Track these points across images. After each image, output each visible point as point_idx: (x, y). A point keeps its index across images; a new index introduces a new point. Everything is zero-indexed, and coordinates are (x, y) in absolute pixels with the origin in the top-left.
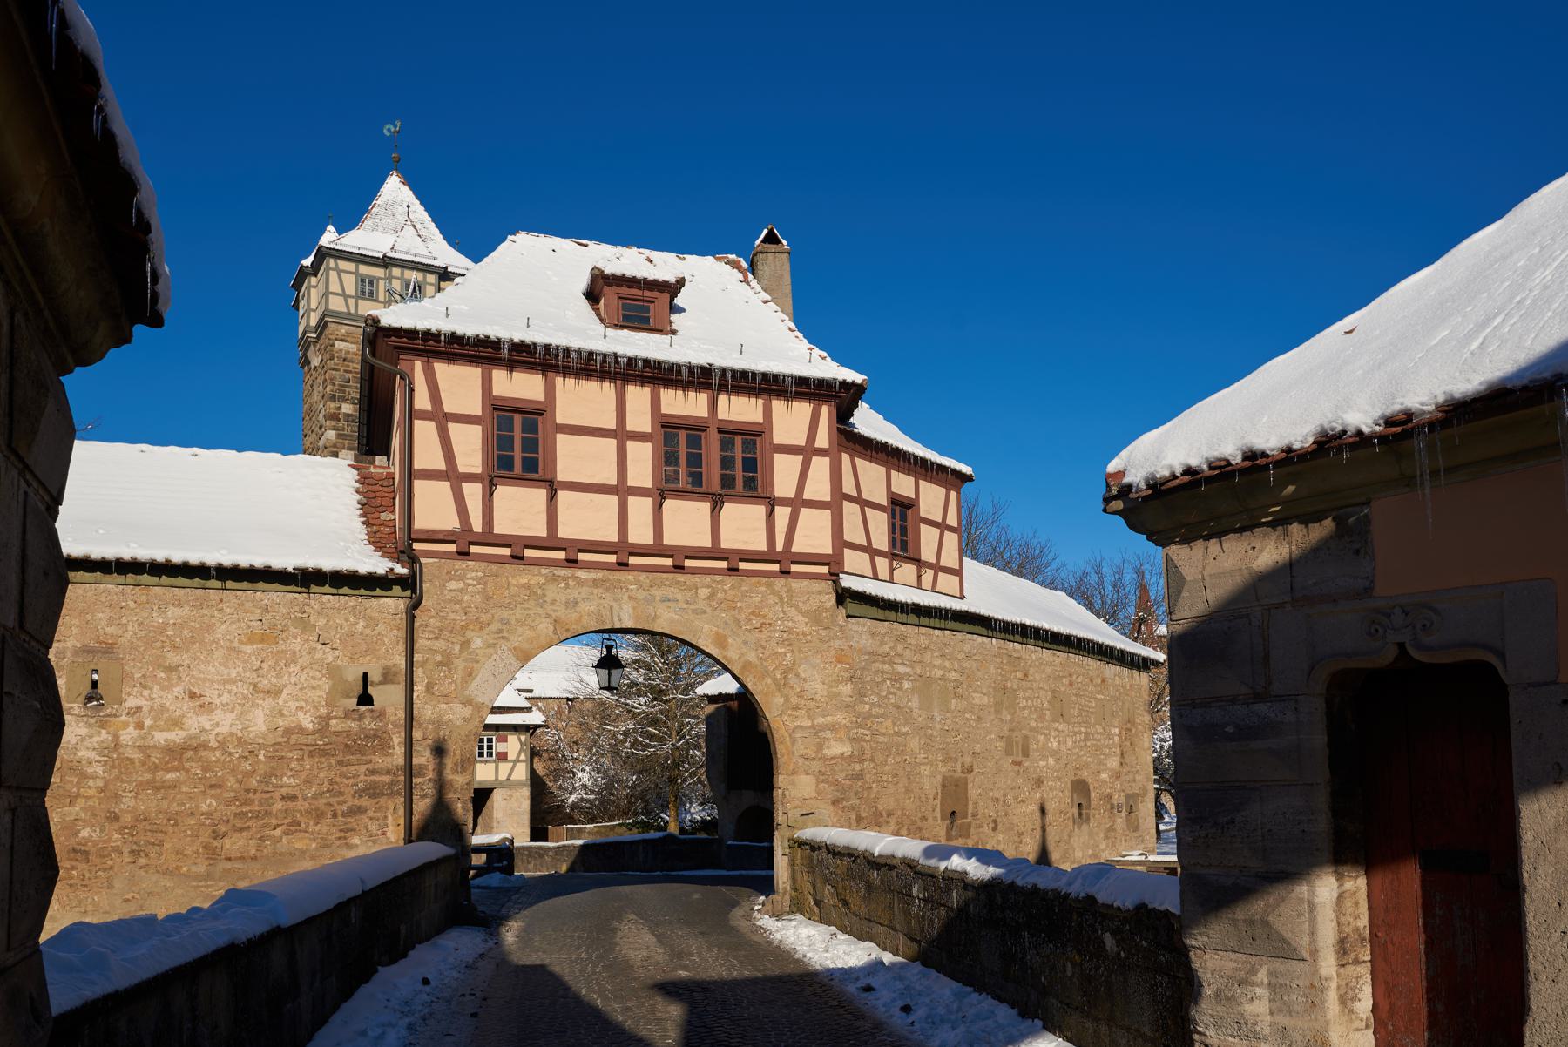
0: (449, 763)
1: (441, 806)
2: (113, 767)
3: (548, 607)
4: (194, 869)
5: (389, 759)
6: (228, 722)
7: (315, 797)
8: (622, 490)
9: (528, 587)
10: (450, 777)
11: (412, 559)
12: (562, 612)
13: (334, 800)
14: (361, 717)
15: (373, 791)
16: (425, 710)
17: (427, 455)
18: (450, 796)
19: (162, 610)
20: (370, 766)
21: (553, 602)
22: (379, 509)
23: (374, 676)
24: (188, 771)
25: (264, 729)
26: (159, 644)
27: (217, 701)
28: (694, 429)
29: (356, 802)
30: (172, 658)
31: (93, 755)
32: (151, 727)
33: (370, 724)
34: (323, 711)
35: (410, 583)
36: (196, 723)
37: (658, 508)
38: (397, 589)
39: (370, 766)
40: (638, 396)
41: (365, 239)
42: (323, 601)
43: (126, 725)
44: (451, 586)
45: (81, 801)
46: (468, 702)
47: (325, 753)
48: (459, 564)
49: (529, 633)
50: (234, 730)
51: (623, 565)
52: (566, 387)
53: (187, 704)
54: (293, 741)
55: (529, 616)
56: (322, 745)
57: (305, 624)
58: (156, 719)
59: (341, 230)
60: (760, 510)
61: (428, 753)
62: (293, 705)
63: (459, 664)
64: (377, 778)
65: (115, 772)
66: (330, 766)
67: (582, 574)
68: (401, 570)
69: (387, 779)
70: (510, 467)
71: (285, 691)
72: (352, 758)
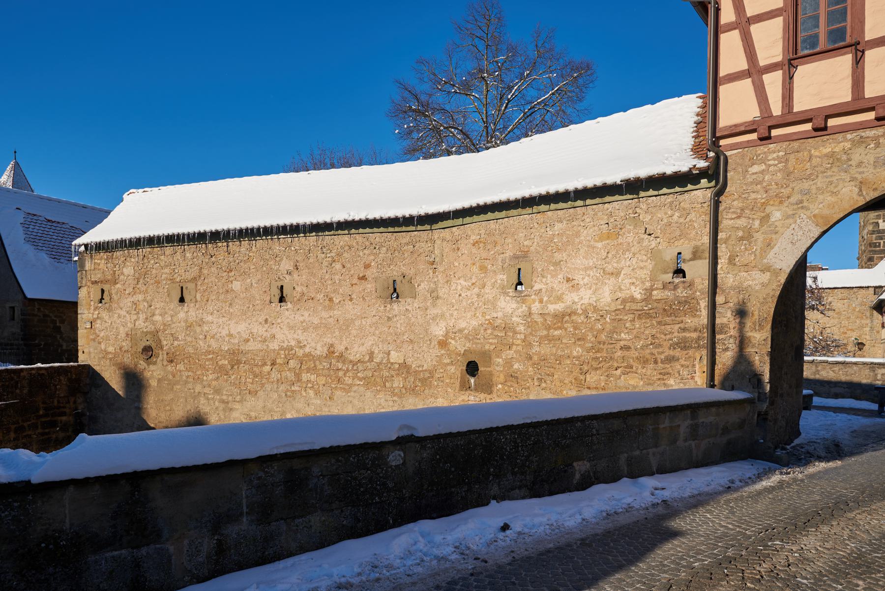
0: (749, 323)
1: (742, 358)
2: (529, 327)
3: (853, 171)
4: (570, 393)
5: (696, 320)
6: (587, 296)
7: (642, 348)
9: (832, 155)
10: (749, 334)
13: (655, 351)
14: (675, 288)
15: (684, 345)
16: (726, 278)
18: (750, 350)
19: (552, 226)
20: (682, 325)
21: (860, 164)
23: (686, 255)
24: (566, 329)
25: (609, 300)
26: (550, 248)
27: (581, 283)
29: (671, 353)
30: (558, 256)
31: (518, 320)
32: (546, 302)
33: (681, 293)
34: (648, 284)
35: (715, 173)
36: (571, 298)
38: (704, 181)
39: (682, 325)
43: (534, 301)
45: (514, 347)
46: (766, 269)
47: (649, 316)
48: (762, 149)
49: (830, 199)
50: (591, 301)
53: (566, 286)
54: (627, 308)
55: (831, 183)
56: (649, 311)
57: (636, 220)
58: (550, 297)
61: (729, 314)
62: (627, 281)
63: (759, 237)
64: (687, 335)
65: (529, 330)
66: (652, 325)
69: (694, 335)
70: (813, 41)
71: (623, 272)
72: (668, 319)
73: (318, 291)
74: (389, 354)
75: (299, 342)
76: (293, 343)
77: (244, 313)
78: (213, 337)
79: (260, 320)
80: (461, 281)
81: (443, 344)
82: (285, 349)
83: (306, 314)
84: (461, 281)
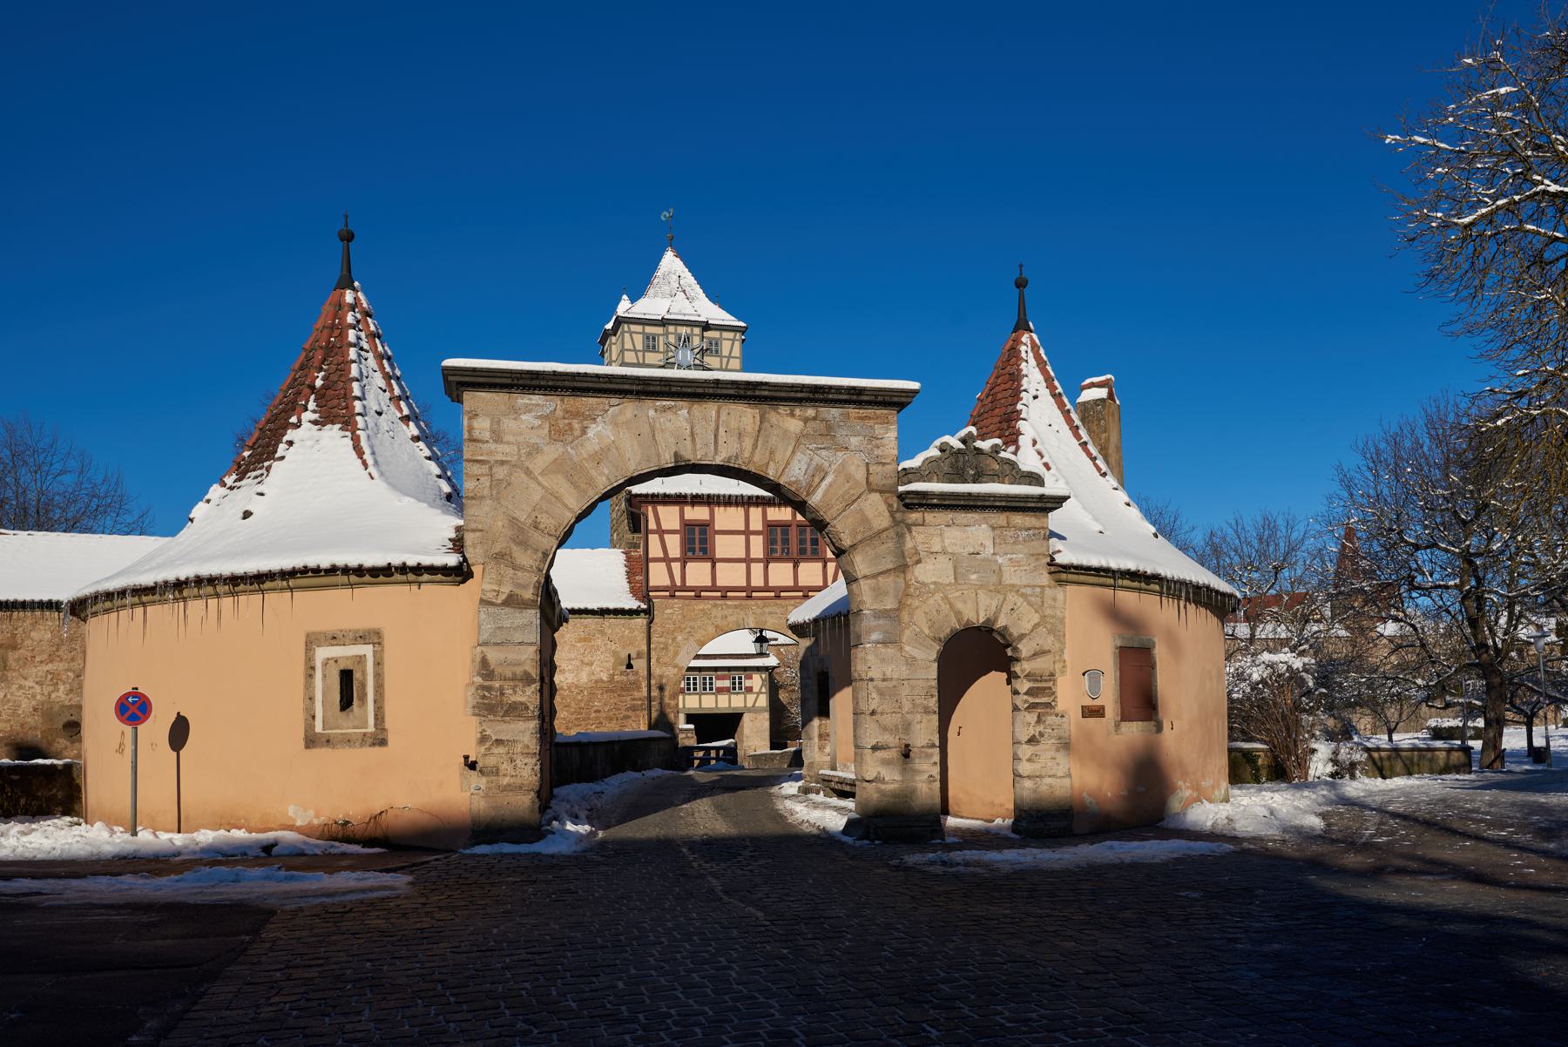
0: (666, 693)
8: (748, 560)
11: (648, 600)
15: (634, 708)
16: (656, 671)
17: (655, 550)
22: (635, 574)
28: (784, 526)
33: (632, 678)
35: (648, 612)
37: (766, 568)
40: (756, 513)
41: (651, 306)
42: (610, 621)
44: (667, 611)
46: (676, 666)
51: (749, 597)
52: (720, 511)
56: (613, 688)
57: (602, 633)
59: (633, 300)
63: (671, 648)
68: (644, 606)
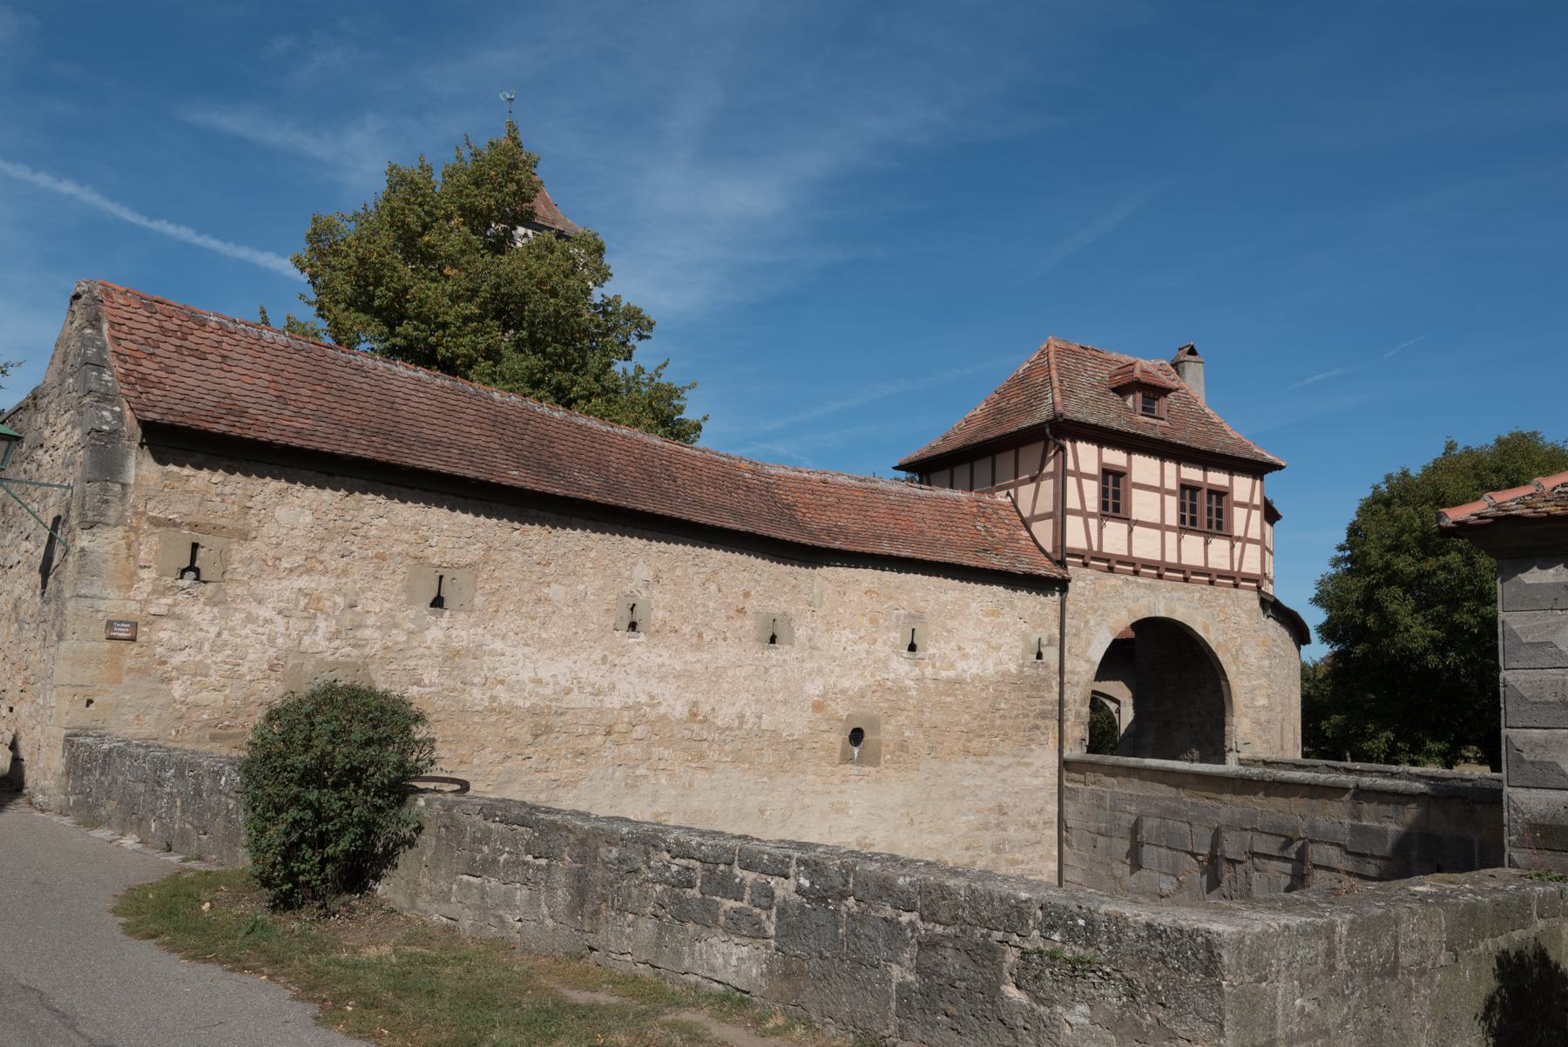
12: (1131, 605)
23: (1044, 641)
30: (950, 624)
31: (911, 683)
36: (961, 665)
40: (1170, 467)
51: (1160, 576)
52: (1137, 459)
53: (957, 654)
60: (1226, 544)
62: (1006, 657)
63: (1083, 635)
67: (1140, 580)
73: (685, 620)
74: (760, 718)
75: (652, 697)
76: (643, 699)
77: (567, 642)
78: (502, 682)
79: (594, 657)
80: (847, 632)
81: (818, 707)
82: (628, 708)
83: (666, 654)
84: (847, 632)
